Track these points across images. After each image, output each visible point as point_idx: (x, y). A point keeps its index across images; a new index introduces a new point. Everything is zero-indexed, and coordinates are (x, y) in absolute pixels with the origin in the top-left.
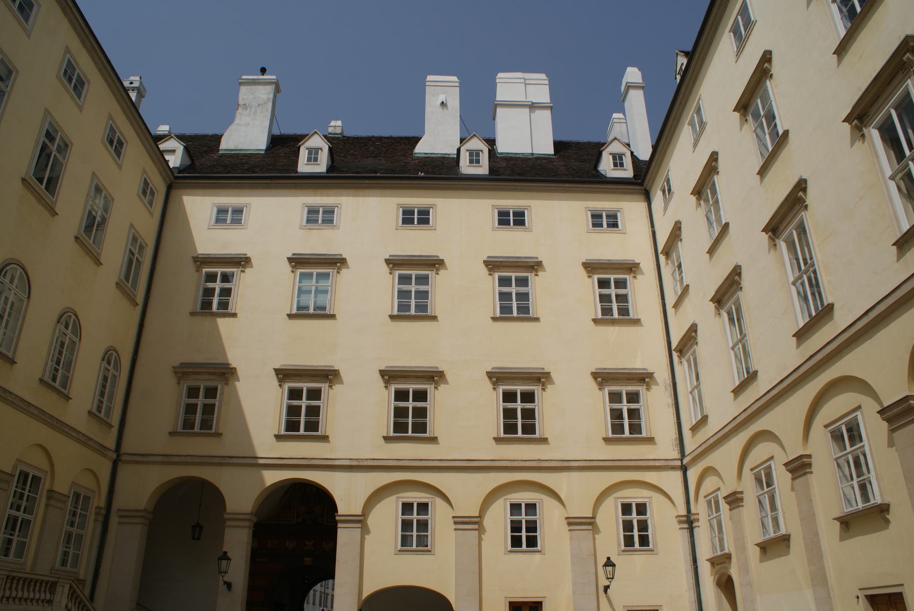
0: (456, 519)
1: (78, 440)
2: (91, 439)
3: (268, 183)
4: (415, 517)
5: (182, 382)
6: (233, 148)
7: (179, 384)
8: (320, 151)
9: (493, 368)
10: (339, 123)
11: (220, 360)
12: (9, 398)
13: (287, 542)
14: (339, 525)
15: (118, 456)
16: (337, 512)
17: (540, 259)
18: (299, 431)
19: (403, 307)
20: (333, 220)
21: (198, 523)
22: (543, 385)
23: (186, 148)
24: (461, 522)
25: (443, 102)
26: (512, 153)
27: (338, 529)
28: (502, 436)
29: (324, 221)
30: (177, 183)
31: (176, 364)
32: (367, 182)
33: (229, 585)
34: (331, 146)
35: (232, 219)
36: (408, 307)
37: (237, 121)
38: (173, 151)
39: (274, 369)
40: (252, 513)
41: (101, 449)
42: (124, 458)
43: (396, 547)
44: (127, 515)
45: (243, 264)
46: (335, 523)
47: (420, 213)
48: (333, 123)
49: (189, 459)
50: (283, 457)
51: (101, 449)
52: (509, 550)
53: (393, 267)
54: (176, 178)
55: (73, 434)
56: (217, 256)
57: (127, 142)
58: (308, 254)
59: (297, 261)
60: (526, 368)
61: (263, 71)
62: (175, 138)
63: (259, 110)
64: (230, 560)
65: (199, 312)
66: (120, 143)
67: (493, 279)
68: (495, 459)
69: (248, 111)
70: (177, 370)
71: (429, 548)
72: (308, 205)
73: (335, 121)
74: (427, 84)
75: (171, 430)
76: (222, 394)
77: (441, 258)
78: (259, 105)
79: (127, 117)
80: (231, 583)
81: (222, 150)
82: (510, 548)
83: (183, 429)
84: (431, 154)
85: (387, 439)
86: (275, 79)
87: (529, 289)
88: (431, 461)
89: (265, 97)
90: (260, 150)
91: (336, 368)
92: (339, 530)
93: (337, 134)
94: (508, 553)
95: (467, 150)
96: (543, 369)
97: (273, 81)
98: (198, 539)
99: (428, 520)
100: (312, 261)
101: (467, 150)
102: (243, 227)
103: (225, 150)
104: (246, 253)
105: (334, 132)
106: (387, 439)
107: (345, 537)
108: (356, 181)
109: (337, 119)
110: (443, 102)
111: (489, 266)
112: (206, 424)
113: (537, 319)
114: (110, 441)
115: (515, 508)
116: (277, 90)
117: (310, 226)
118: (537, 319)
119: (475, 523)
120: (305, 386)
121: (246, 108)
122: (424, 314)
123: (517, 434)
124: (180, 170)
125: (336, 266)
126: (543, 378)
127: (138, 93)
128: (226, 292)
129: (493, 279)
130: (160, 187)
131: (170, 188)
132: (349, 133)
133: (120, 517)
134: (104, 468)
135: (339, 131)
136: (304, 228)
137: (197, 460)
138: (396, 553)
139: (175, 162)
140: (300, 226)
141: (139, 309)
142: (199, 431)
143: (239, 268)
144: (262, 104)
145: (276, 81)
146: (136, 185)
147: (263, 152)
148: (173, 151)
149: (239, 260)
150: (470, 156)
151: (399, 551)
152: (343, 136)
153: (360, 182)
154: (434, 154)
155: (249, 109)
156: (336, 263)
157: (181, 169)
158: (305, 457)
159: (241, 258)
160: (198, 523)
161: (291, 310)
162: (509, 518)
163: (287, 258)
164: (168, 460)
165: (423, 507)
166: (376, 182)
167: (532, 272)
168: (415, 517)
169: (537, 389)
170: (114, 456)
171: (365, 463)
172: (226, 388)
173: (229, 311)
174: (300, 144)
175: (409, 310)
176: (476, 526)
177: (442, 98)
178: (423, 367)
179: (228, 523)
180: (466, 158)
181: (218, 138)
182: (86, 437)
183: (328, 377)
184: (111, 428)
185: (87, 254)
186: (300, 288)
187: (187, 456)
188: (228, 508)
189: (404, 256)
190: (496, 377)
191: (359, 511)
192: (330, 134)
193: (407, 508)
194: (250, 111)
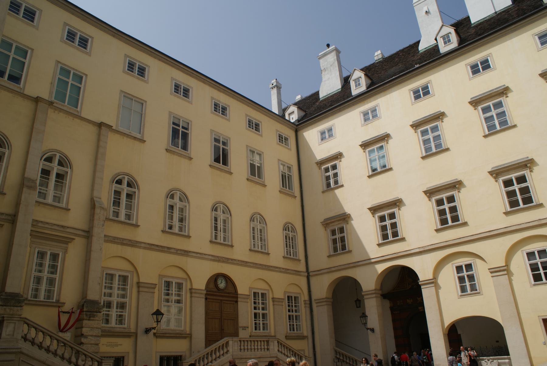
0: (491, 270)
1: (281, 272)
2: (288, 270)
4: (465, 274)
5: (327, 228)
6: (326, 95)
7: (326, 230)
8: (360, 79)
9: (492, 168)
10: (379, 52)
11: (342, 212)
12: (235, 262)
13: (408, 300)
14: (422, 287)
15: (308, 273)
16: (419, 280)
17: (507, 86)
18: (389, 239)
19: (428, 149)
20: (377, 115)
21: (358, 299)
22: (530, 168)
24: (494, 271)
25: (426, 12)
26: (481, 20)
27: (422, 289)
28: (509, 210)
30: (299, 128)
31: (322, 220)
32: (388, 85)
34: (365, 73)
36: (430, 148)
37: (324, 79)
39: (368, 209)
40: (375, 290)
41: (297, 273)
42: (311, 274)
43: (458, 294)
44: (319, 301)
46: (419, 287)
47: (423, 89)
48: (376, 54)
49: (340, 268)
51: (297, 273)
52: (533, 284)
53: (416, 128)
54: (297, 125)
55: (277, 270)
57: (261, 122)
58: (369, 139)
59: (365, 145)
60: (515, 161)
61: (328, 46)
63: (332, 68)
65: (326, 190)
66: (257, 125)
67: (478, 111)
68: (508, 226)
69: (327, 72)
70: (323, 224)
71: (478, 291)
72: (363, 112)
73: (377, 52)
74: (414, 6)
75: (328, 255)
76: (347, 230)
77: (442, 111)
78: (331, 65)
79: (257, 110)
80: (373, 329)
81: (321, 98)
82: (533, 282)
83: (334, 253)
84: (429, 47)
85: (437, 231)
86: (334, 48)
87: (504, 109)
88: (466, 238)
89: (332, 59)
90: (339, 89)
92: (423, 290)
93: (380, 59)
94: (533, 286)
95: (441, 37)
96: (528, 157)
97: (333, 49)
98: (360, 307)
99: (473, 274)
101: (441, 37)
102: (334, 138)
103: (323, 97)
105: (378, 59)
106: (437, 231)
107: (427, 293)
109: (377, 51)
110: (426, 12)
111: (473, 104)
112: (344, 247)
113: (515, 126)
114: (302, 267)
115: (531, 255)
116: (338, 52)
117: (367, 123)
118: (515, 126)
119: (504, 270)
120: (386, 213)
121: (326, 70)
122: (442, 150)
123: (520, 206)
124: (298, 121)
125: (385, 140)
126: (528, 164)
127: (277, 87)
128: (336, 175)
129: (478, 111)
130: (289, 133)
131: (296, 132)
132: (387, 55)
133: (317, 303)
134: (303, 282)
135: (380, 57)
136: (364, 125)
137: (343, 267)
138: (459, 298)
139: (295, 117)
140: (362, 125)
143: (338, 160)
144: (332, 64)
145: (335, 48)
146: (275, 139)
147: (340, 90)
149: (337, 156)
150: (443, 40)
151: (460, 296)
152: (383, 59)
153: (384, 86)
154: (431, 46)
155: (327, 70)
156: (385, 138)
158: (396, 252)
159: (337, 154)
160: (358, 299)
161: (369, 173)
162: (528, 263)
163: (360, 145)
164: (330, 270)
165: (469, 267)
167: (503, 96)
168: (465, 274)
169: (526, 172)
170: (306, 274)
171: (427, 248)
172: (348, 226)
173: (339, 184)
174: (349, 80)
176: (505, 272)
177: (425, 9)
178: (448, 181)
179: (365, 297)
180: (442, 43)
181: (317, 93)
182: (285, 269)
184: (300, 261)
185: (257, 184)
186: (370, 160)
188: (363, 290)
189: (421, 119)
190: (496, 173)
191: (431, 277)
192: (376, 61)
193: (459, 269)
194: (328, 71)
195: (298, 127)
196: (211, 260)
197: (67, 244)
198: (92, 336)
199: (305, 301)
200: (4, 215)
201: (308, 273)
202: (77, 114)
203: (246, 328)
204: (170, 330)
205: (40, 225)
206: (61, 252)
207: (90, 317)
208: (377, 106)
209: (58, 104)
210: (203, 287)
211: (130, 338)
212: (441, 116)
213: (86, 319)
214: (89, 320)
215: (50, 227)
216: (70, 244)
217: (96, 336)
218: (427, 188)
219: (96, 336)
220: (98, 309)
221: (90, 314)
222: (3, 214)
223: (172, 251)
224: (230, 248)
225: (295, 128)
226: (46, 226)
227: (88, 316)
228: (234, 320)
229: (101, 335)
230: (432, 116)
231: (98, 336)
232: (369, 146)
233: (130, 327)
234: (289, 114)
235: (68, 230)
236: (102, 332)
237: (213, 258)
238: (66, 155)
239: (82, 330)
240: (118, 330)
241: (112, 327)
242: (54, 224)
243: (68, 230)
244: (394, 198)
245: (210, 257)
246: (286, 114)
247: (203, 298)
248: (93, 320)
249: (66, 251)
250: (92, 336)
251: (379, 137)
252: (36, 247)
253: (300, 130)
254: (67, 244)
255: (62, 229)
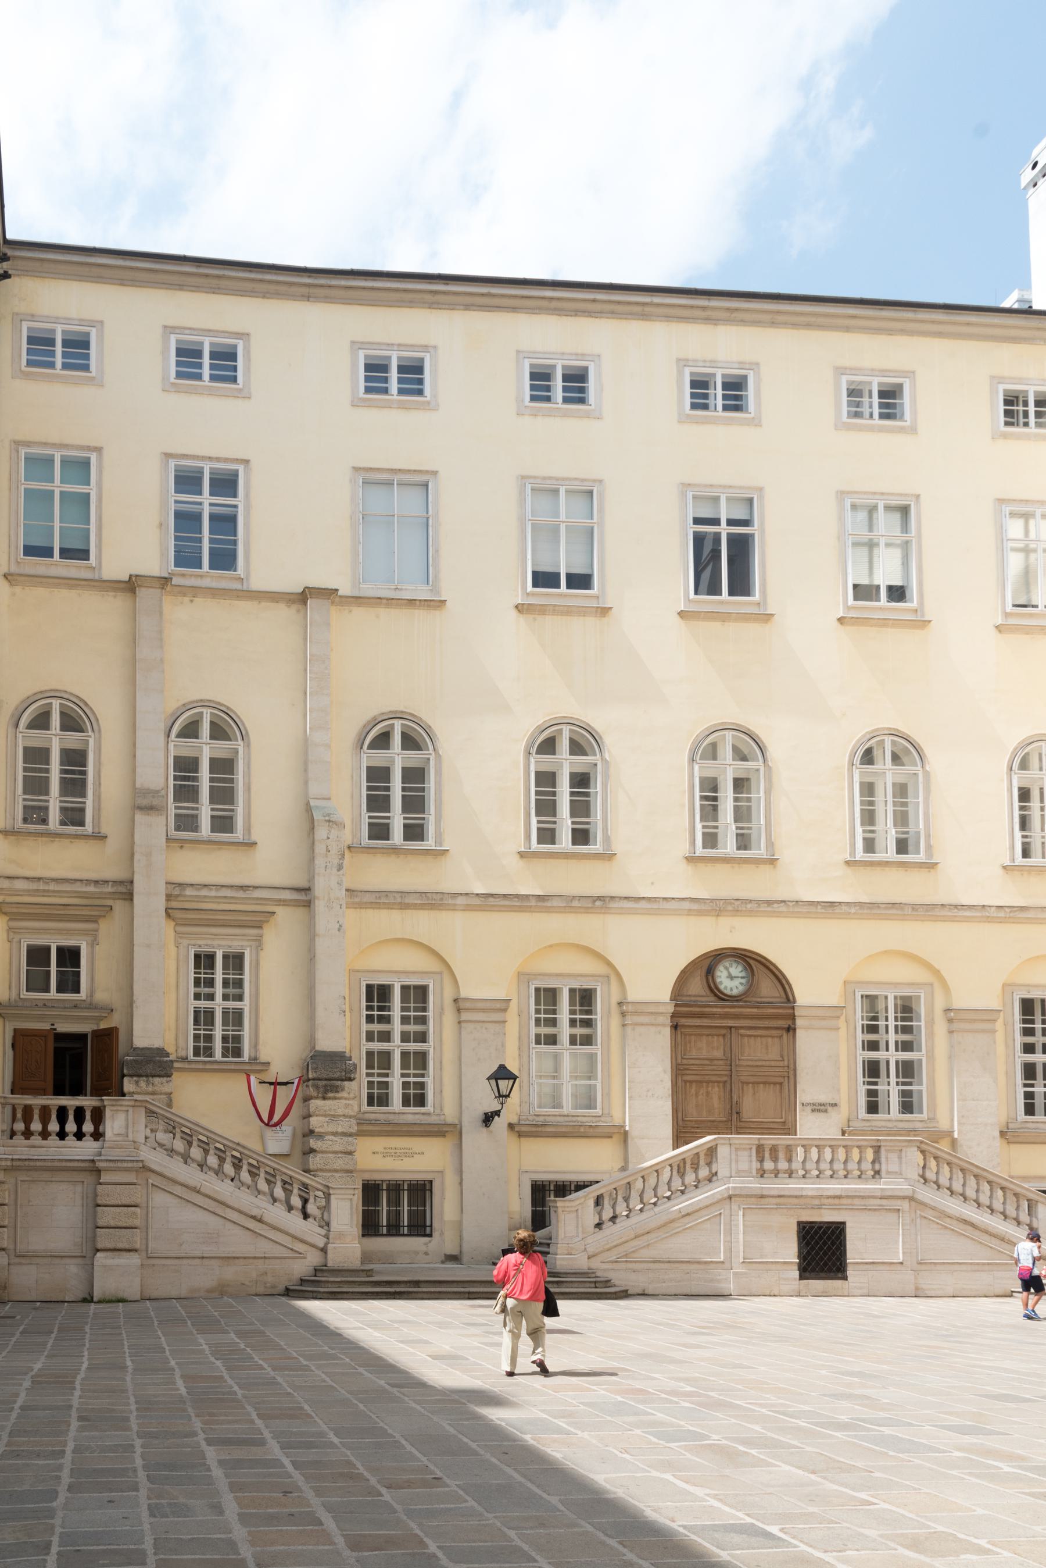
196: (690, 912)
197: (260, 927)
198: (335, 1134)
200: (110, 883)
202: (238, 586)
203: (830, 1109)
204: (560, 1116)
205: (189, 892)
206: (248, 949)
207: (326, 1092)
209: (188, 577)
210: (664, 994)
211: (444, 1136)
213: (317, 1098)
214: (324, 1098)
215: (213, 893)
216: (265, 926)
217: (344, 1134)
219: (344, 1134)
220: (344, 1074)
221: (326, 1086)
222: (108, 882)
223: (555, 903)
224: (766, 868)
226: (204, 892)
227: (321, 1090)
228: (781, 1084)
229: (358, 1131)
231: (351, 1135)
233: (441, 1110)
235: (257, 894)
236: (358, 1124)
237: (695, 906)
238: (228, 708)
239: (309, 1122)
240: (410, 1118)
241: (394, 1113)
242: (223, 886)
243: (257, 894)
245: (686, 905)
247: (664, 1025)
248: (335, 1098)
249: (258, 943)
250: (335, 1134)
252: (189, 945)
254: (260, 927)
255: (241, 894)
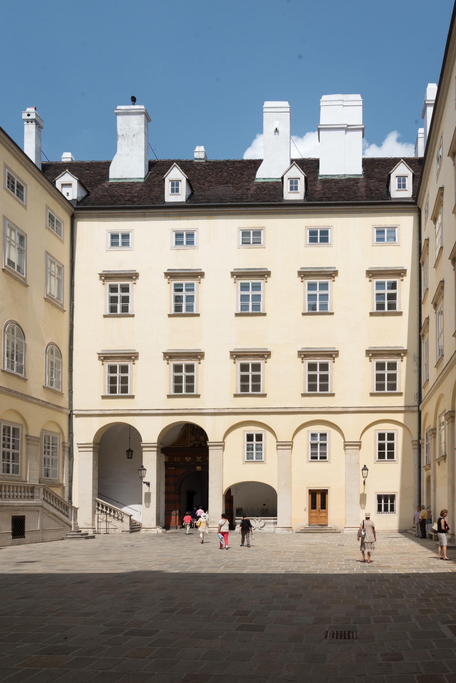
3: (144, 212)
23: (79, 182)
29: (188, 243)
32: (215, 209)
33: (148, 484)
35: (123, 242)
38: (70, 185)
42: (74, 412)
45: (134, 278)
50: (174, 408)
56: (115, 273)
62: (70, 173)
64: (146, 470)
91: (203, 351)
100: (181, 275)
104: (135, 270)
108: (207, 210)
141: (67, 314)
142: (120, 394)
148: (70, 185)
153: (210, 210)
157: (79, 200)
159: (132, 274)
166: (221, 209)
175: (248, 310)
183: (197, 357)
184: (63, 395)
187: (114, 410)
195: (76, 212)
199: (63, 443)
201: (72, 411)
208: (196, 231)
212: (266, 275)
218: (235, 349)
225: (72, 212)
230: (257, 271)
232: (177, 278)
234: (63, 185)
244: (196, 350)
246: (57, 181)
251: (191, 271)
253: (79, 217)
